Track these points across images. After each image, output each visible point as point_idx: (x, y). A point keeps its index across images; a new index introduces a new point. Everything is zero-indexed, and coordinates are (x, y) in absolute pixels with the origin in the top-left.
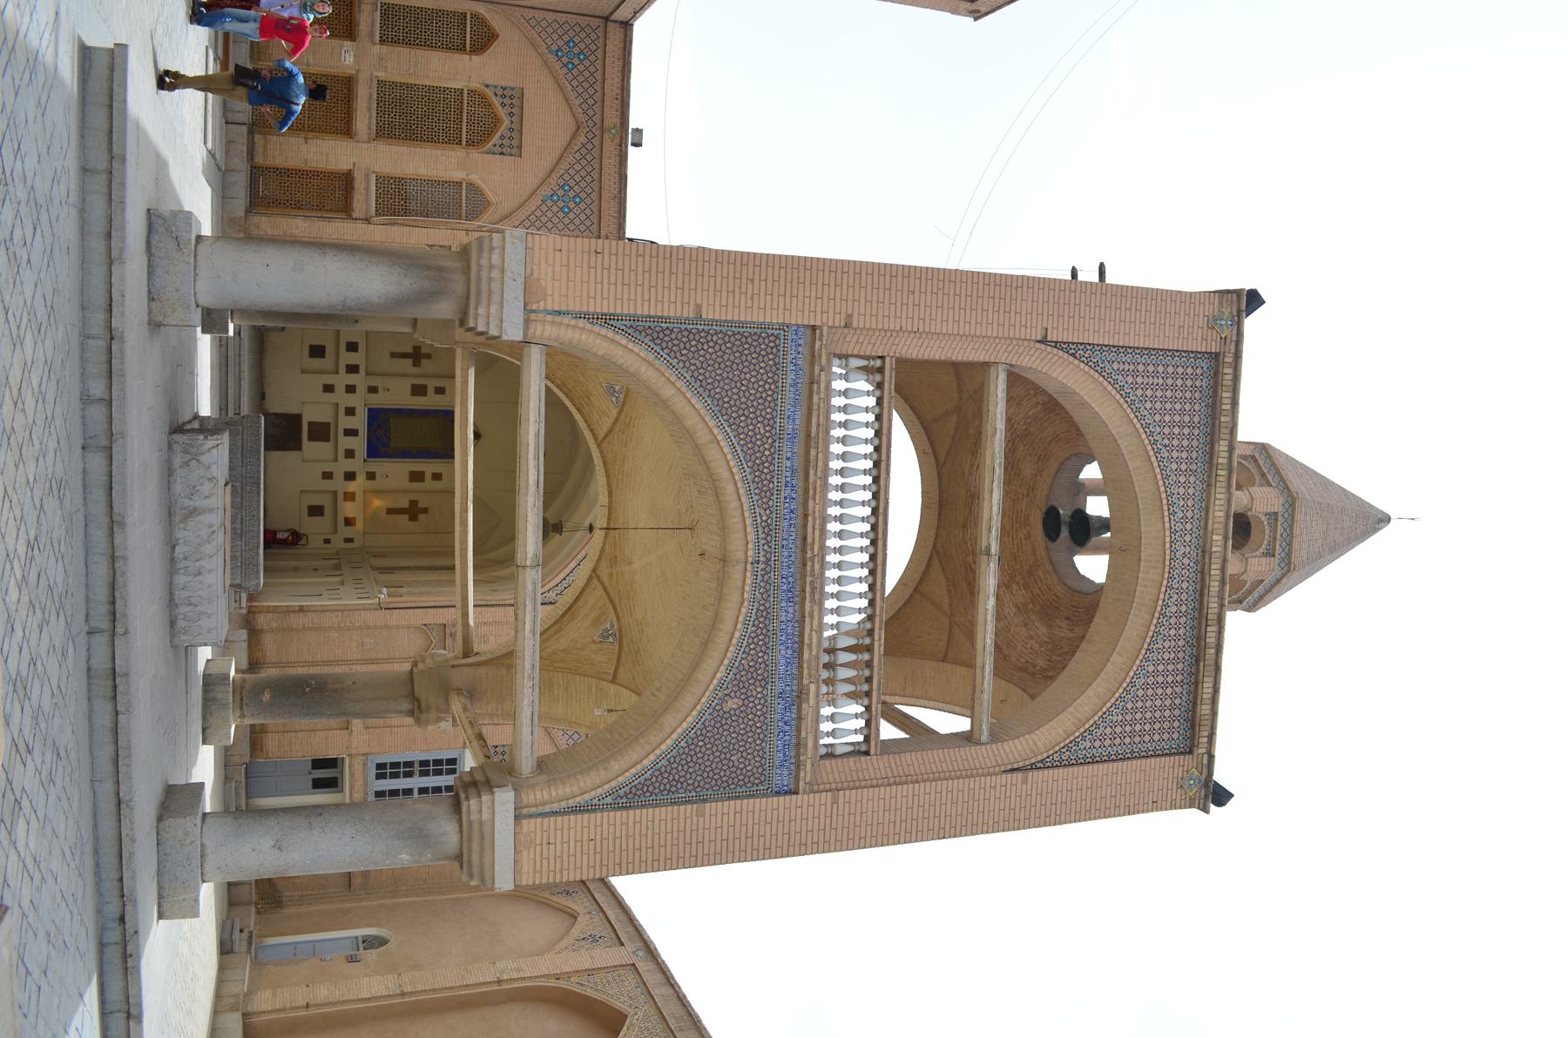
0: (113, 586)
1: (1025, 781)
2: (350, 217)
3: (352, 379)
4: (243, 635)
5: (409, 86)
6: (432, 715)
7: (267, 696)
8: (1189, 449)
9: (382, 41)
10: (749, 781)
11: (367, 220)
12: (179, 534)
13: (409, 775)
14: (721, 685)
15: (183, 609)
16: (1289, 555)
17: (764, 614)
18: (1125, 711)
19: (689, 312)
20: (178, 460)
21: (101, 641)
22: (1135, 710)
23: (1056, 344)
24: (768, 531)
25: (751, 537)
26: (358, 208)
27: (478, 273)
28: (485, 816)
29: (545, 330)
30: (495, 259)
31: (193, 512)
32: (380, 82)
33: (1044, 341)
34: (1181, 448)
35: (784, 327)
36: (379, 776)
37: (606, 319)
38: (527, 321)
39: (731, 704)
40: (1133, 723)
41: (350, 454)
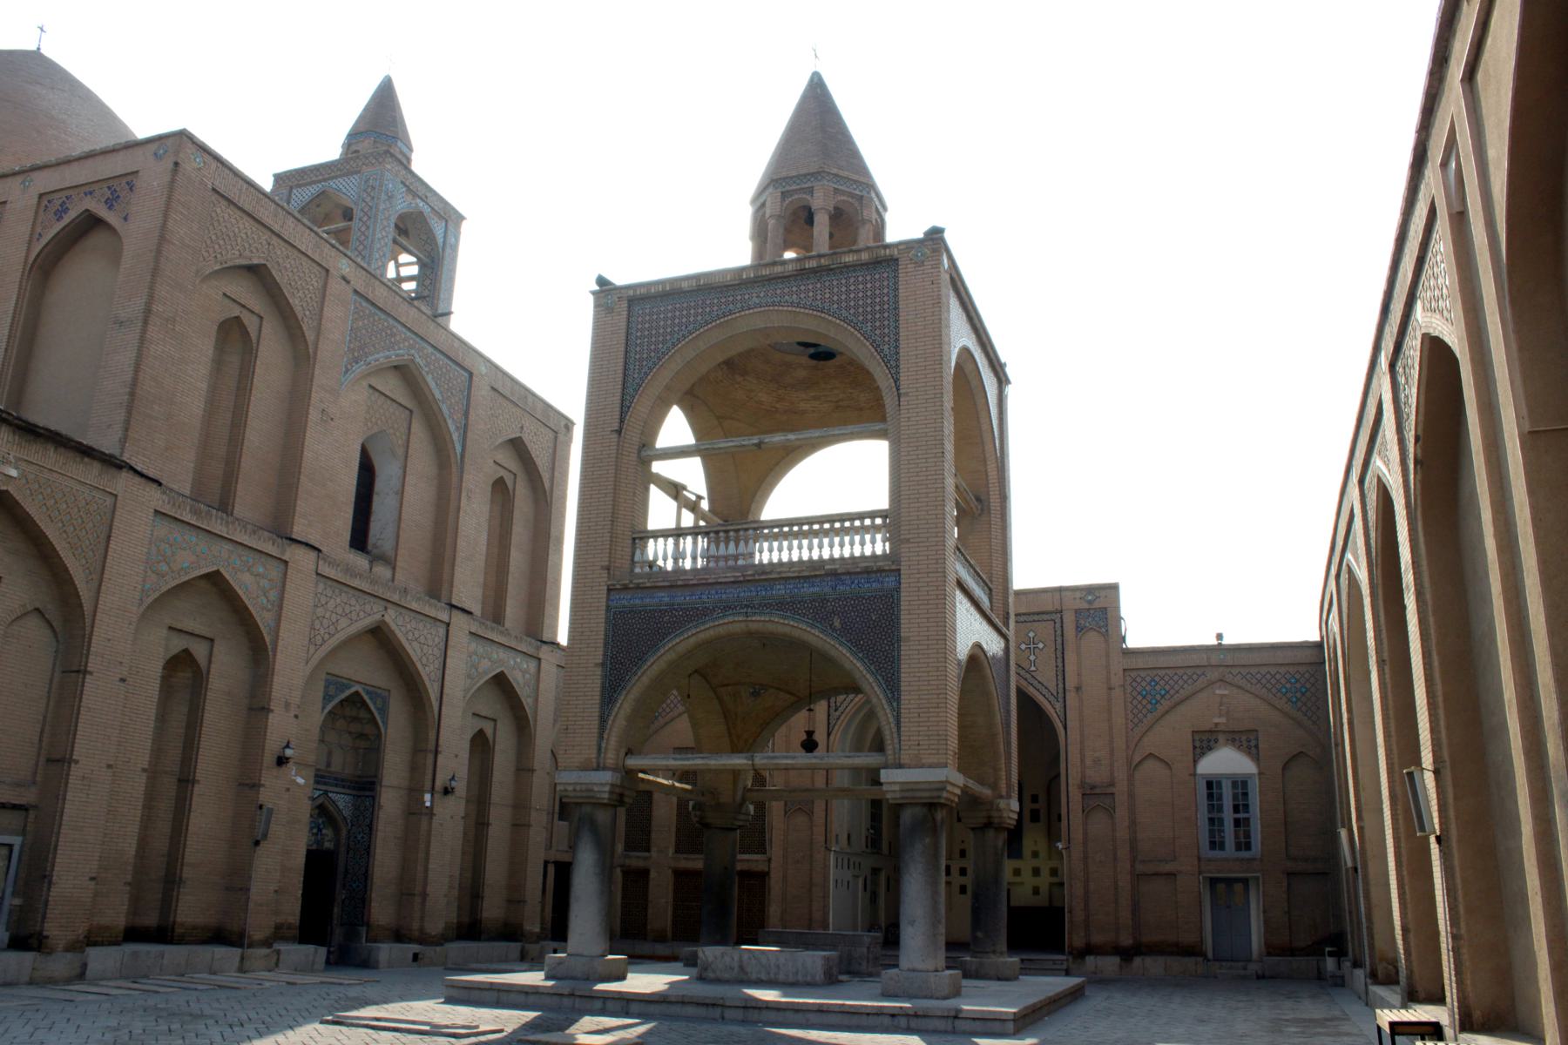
0: (698, 1004)
1: (907, 394)
2: (768, 873)
3: (1045, 872)
4: (1090, 959)
5: (678, 830)
6: (995, 814)
7: (979, 934)
8: (688, 309)
9: (648, 850)
10: (888, 605)
11: (769, 860)
12: (754, 976)
13: (1221, 821)
14: (823, 631)
15: (800, 978)
16: (812, 174)
17: (781, 606)
18: (865, 321)
19: (599, 671)
20: (711, 975)
21: (729, 1014)
22: (865, 313)
23: (622, 422)
24: (728, 608)
25: (731, 619)
26: (762, 867)
27: (414, 812)
28: (897, 788)
29: (610, 758)
30: (570, 788)
31: (741, 968)
32: (678, 851)
33: (619, 432)
34: (688, 315)
35: (608, 608)
36: (1222, 846)
37: (603, 720)
38: (605, 768)
39: (837, 624)
40: (873, 313)
41: (1017, 872)
